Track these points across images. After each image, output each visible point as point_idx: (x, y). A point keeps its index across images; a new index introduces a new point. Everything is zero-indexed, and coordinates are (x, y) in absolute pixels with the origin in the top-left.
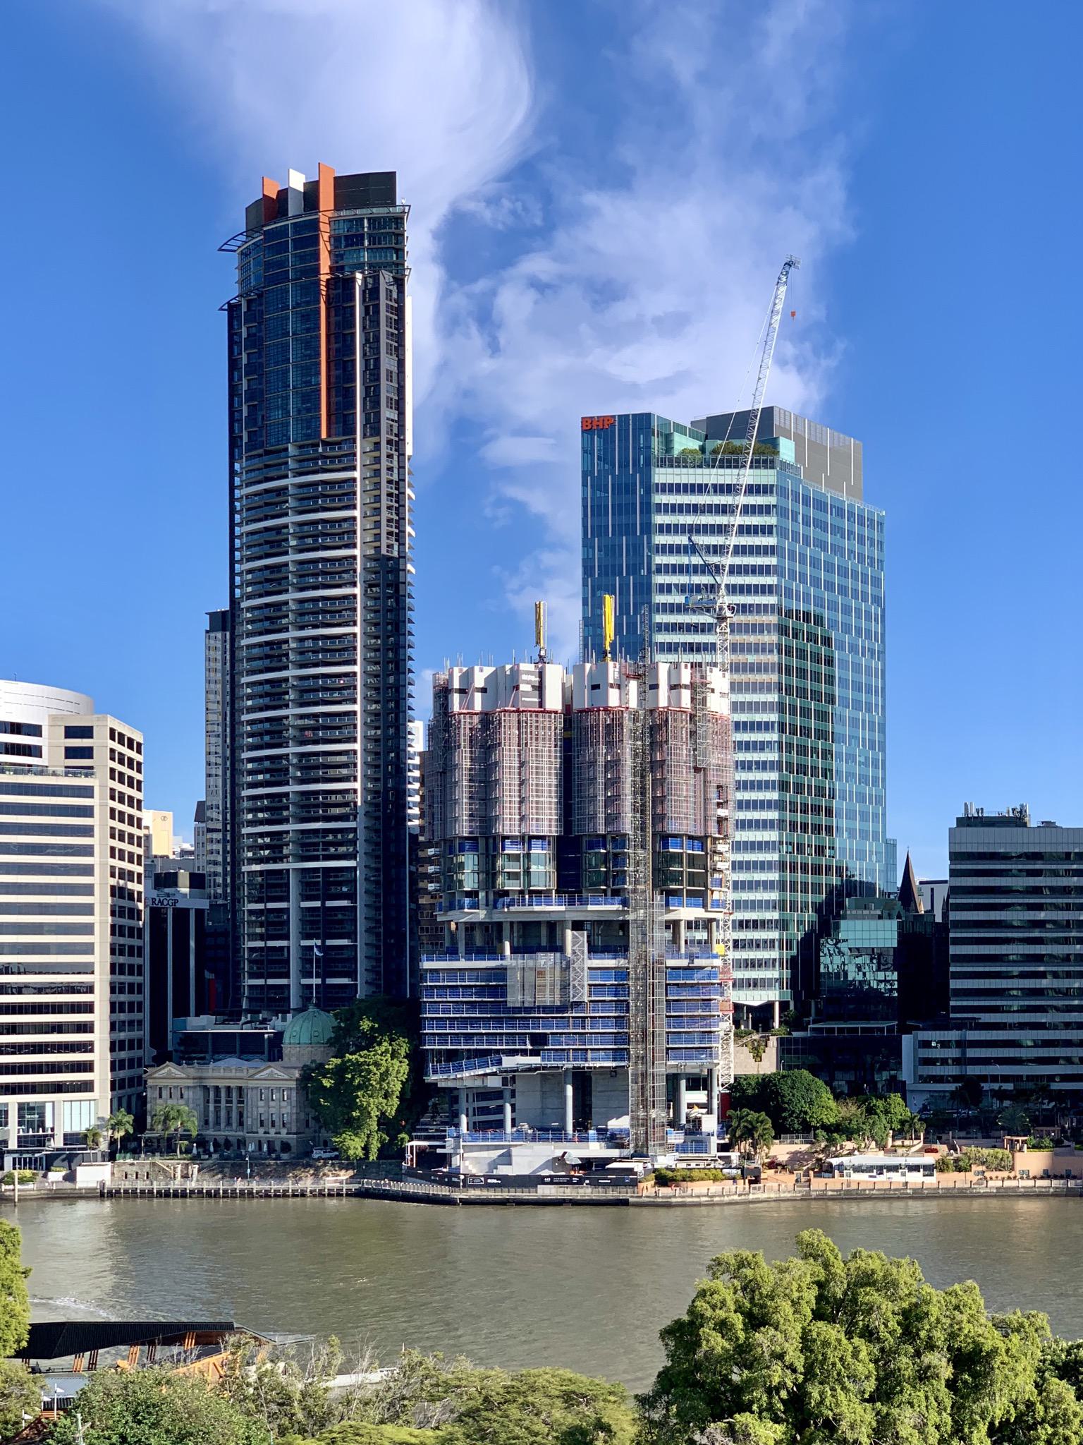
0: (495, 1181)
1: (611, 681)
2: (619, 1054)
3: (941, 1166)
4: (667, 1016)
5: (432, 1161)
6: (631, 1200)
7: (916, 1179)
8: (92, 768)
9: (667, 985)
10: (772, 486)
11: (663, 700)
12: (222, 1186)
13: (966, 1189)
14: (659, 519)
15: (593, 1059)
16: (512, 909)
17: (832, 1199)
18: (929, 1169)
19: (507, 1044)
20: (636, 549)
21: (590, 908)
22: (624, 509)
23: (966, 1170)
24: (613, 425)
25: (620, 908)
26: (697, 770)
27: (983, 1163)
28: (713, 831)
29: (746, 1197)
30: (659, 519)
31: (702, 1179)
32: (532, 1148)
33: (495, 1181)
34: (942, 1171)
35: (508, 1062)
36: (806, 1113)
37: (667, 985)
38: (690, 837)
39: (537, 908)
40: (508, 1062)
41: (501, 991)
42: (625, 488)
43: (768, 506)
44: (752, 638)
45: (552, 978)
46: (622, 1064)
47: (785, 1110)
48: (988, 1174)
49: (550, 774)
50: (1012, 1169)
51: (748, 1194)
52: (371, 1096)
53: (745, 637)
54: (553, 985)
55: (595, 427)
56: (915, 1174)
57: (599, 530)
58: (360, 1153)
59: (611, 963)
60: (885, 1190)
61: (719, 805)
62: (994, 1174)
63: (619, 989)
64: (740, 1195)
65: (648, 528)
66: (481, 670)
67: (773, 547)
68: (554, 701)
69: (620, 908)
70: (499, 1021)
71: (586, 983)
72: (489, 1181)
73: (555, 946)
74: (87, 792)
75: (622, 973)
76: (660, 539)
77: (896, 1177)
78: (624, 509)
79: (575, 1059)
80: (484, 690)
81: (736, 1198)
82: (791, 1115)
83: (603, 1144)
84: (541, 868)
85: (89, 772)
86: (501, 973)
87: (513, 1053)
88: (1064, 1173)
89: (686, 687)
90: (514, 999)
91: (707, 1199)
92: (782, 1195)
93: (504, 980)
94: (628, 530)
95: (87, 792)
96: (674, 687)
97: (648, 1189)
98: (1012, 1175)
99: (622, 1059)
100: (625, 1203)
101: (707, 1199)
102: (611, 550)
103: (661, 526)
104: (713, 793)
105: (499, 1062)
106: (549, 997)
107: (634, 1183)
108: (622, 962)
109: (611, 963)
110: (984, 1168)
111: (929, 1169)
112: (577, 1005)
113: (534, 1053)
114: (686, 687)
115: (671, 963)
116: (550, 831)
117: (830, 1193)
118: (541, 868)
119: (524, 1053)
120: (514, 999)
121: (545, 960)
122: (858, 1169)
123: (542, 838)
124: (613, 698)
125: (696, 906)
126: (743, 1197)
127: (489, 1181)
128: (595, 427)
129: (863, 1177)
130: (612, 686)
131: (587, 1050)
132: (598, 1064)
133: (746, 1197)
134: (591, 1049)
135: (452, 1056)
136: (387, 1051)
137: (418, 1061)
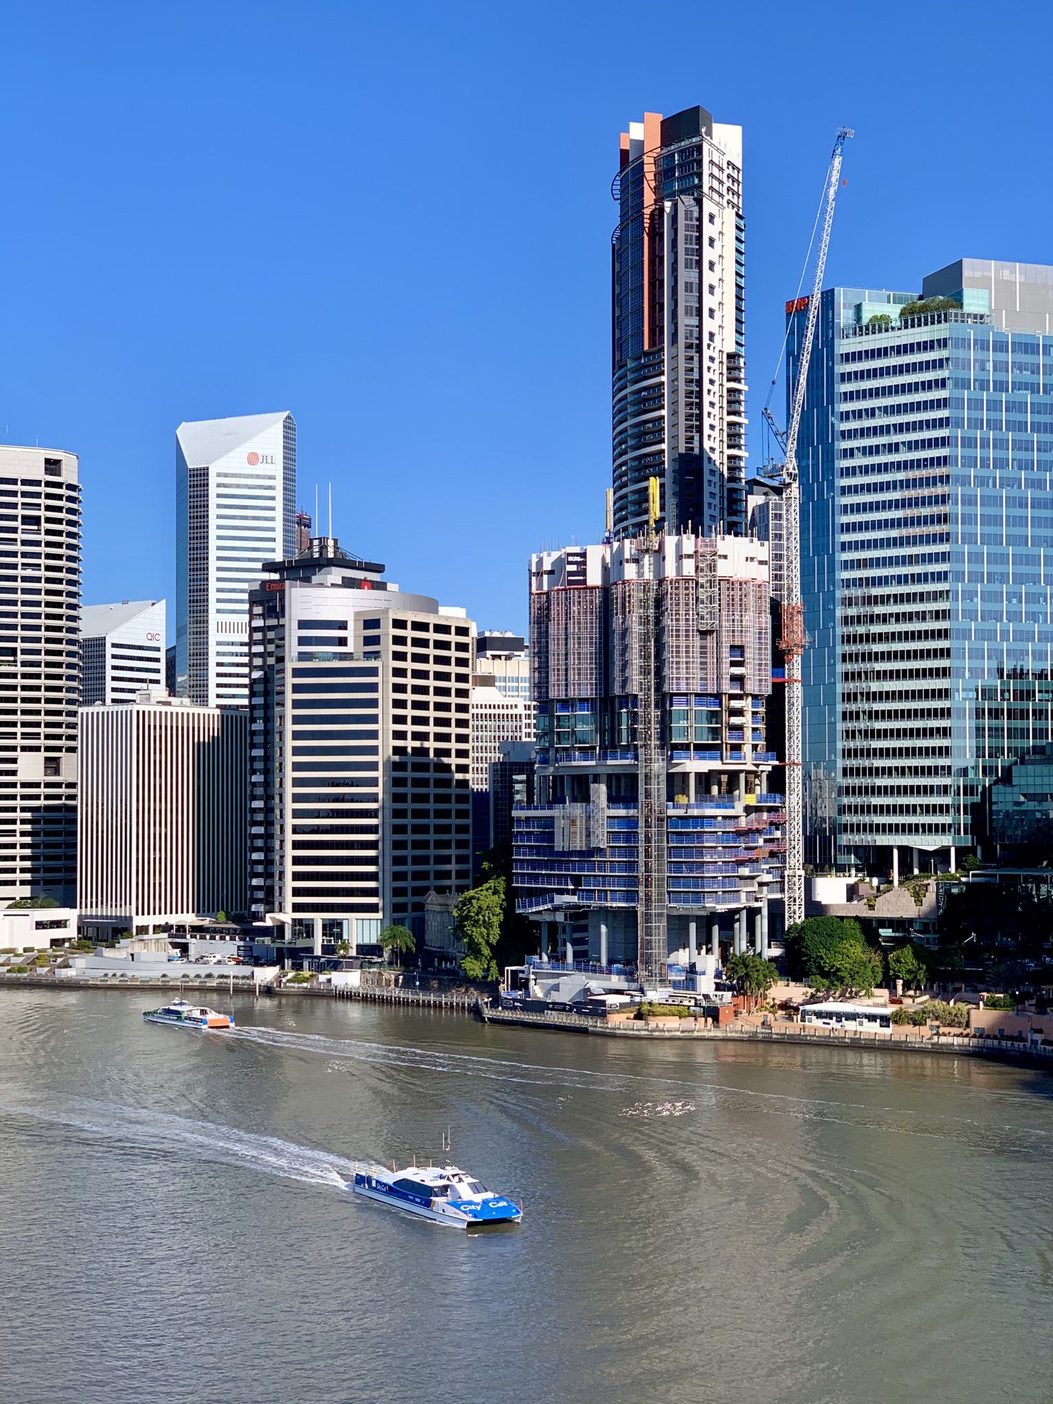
1: (627, 556)
2: (631, 896)
3: (897, 1019)
4: (669, 862)
5: (520, 983)
6: (590, 1029)
7: (872, 1029)
8: (378, 652)
9: (668, 833)
10: (945, 340)
11: (670, 571)
12: (411, 997)
13: (902, 1042)
15: (613, 900)
16: (561, 764)
17: (777, 1042)
18: (885, 1020)
19: (558, 884)
21: (609, 762)
23: (920, 1024)
25: (633, 762)
26: (704, 634)
27: (937, 1018)
28: (727, 688)
29: (690, 1034)
31: (664, 1015)
34: (896, 1022)
35: (560, 900)
36: (821, 958)
37: (668, 833)
38: (697, 695)
39: (574, 763)
40: (560, 900)
41: (550, 837)
43: (941, 360)
44: (926, 492)
45: (580, 826)
46: (632, 905)
47: (804, 954)
48: (942, 1030)
49: (591, 643)
50: (968, 1025)
51: (693, 1031)
52: (473, 926)
53: (919, 491)
54: (581, 832)
56: (853, 1023)
58: (480, 974)
59: (622, 812)
60: (825, 1037)
61: (733, 664)
62: (947, 1030)
63: (631, 836)
64: (682, 1032)
66: (549, 555)
67: (945, 399)
68: (594, 578)
69: (633, 762)
70: (546, 864)
71: (605, 831)
73: (583, 796)
74: (373, 672)
75: (631, 822)
77: (851, 1026)
79: (600, 899)
80: (551, 572)
81: (678, 1034)
82: (809, 960)
83: (623, 977)
84: (586, 728)
85: (376, 655)
86: (550, 821)
87: (561, 892)
88: (1016, 1034)
89: (689, 556)
90: (559, 845)
91: (647, 1033)
92: (729, 1035)
93: (553, 827)
95: (373, 672)
96: (680, 557)
97: (618, 1021)
98: (965, 1032)
99: (633, 900)
100: (584, 1031)
101: (647, 1033)
104: (726, 652)
105: (552, 900)
106: (579, 844)
107: (603, 1015)
108: (632, 812)
109: (622, 812)
110: (936, 1023)
111: (885, 1020)
112: (600, 851)
113: (574, 892)
114: (689, 556)
115: (671, 812)
116: (592, 694)
117: (775, 1036)
118: (586, 728)
119: (567, 892)
120: (559, 845)
121: (577, 810)
122: (819, 1015)
123: (586, 700)
124: (630, 571)
125: (715, 759)
126: (686, 1034)
129: (818, 1023)
130: (627, 561)
131: (606, 891)
132: (614, 905)
133: (690, 1034)
134: (611, 891)
135: (531, 893)
136: (490, 888)
137: (512, 894)
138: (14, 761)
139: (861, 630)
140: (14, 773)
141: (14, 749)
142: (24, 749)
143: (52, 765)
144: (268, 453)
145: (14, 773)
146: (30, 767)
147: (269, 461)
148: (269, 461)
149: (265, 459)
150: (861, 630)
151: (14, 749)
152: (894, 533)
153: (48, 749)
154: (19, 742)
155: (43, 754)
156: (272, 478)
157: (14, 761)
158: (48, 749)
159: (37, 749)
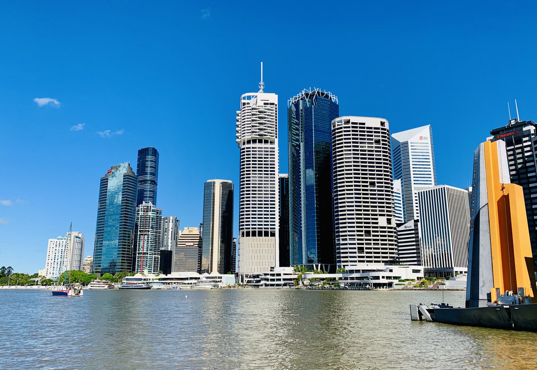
138: (377, 219)
140: (377, 223)
141: (376, 215)
142: (380, 215)
143: (389, 221)
144: (426, 136)
145: (377, 223)
146: (382, 221)
147: (426, 138)
148: (426, 138)
149: (425, 138)
151: (376, 215)
153: (388, 215)
154: (378, 213)
155: (386, 217)
156: (427, 143)
157: (377, 219)
158: (388, 215)
159: (384, 215)
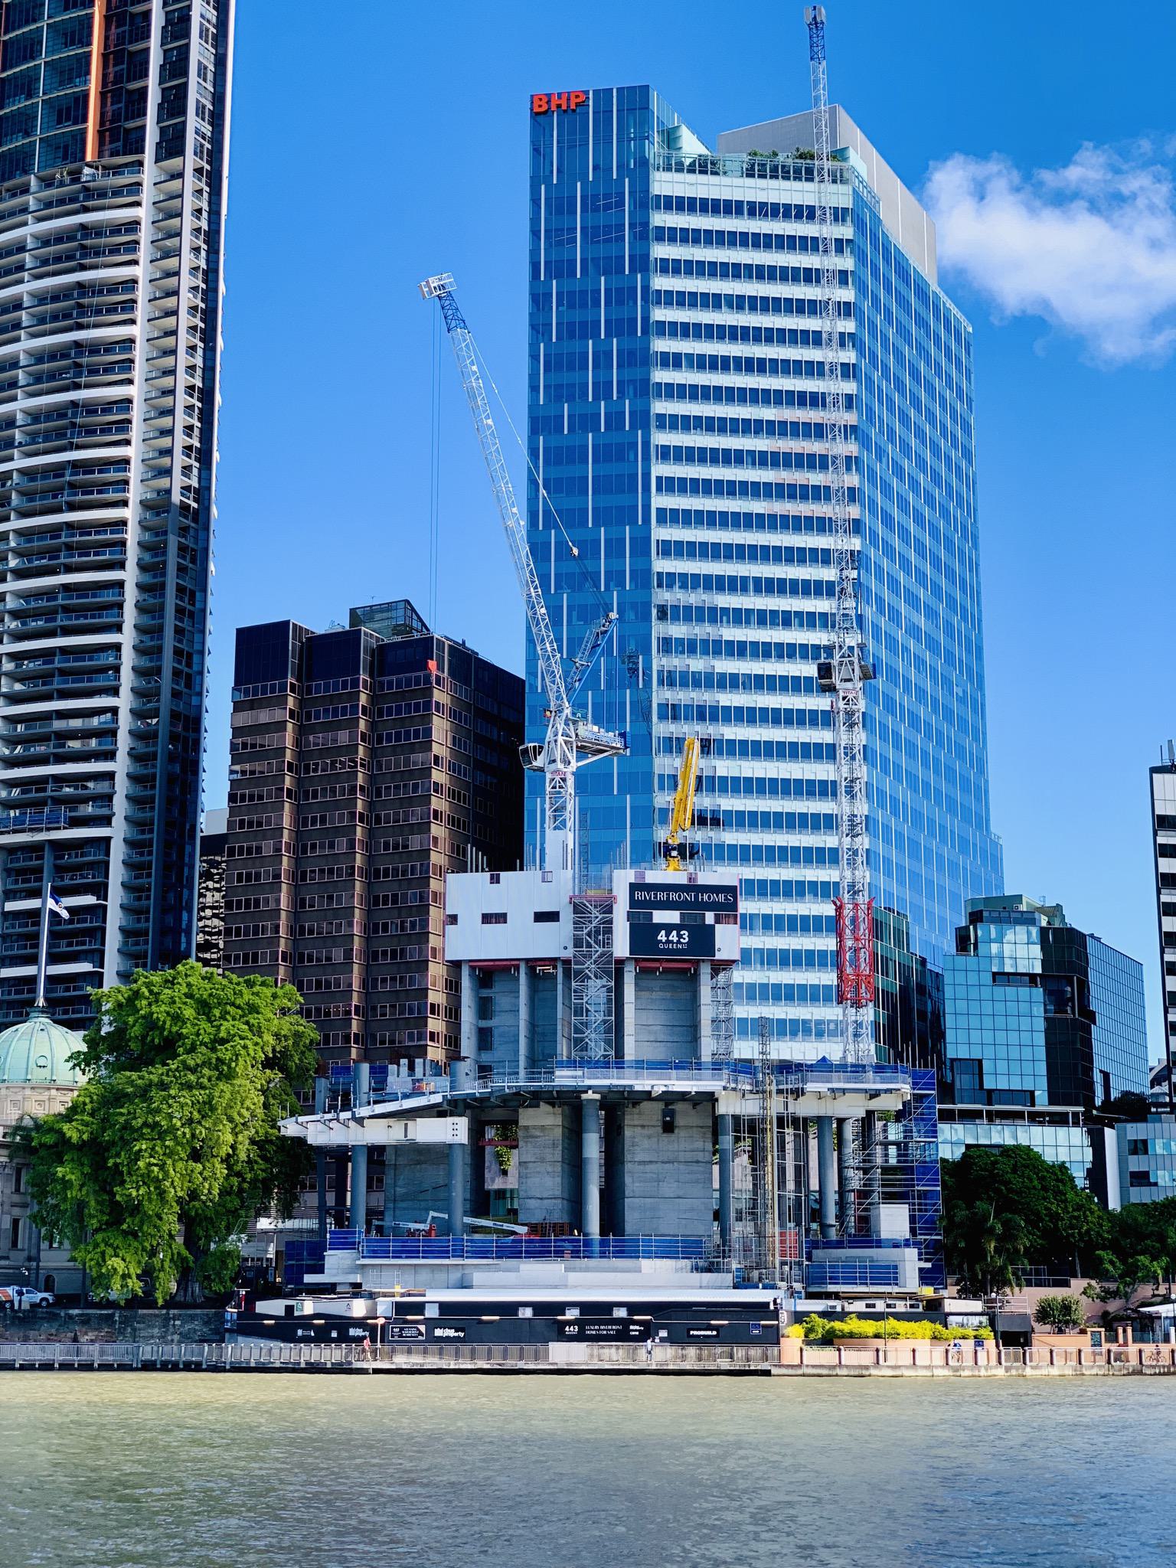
0: (451, 1333)
14: (661, 251)
20: (622, 296)
22: (603, 234)
24: (583, 104)
30: (661, 251)
32: (517, 1270)
33: (451, 1333)
42: (602, 201)
55: (554, 108)
57: (561, 269)
58: (136, 1285)
65: (642, 263)
72: (438, 1332)
76: (661, 283)
78: (603, 234)
94: (613, 266)
102: (579, 299)
103: (664, 261)
127: (438, 1332)
128: (554, 108)
139: (697, 664)
150: (697, 664)
152: (758, 507)
